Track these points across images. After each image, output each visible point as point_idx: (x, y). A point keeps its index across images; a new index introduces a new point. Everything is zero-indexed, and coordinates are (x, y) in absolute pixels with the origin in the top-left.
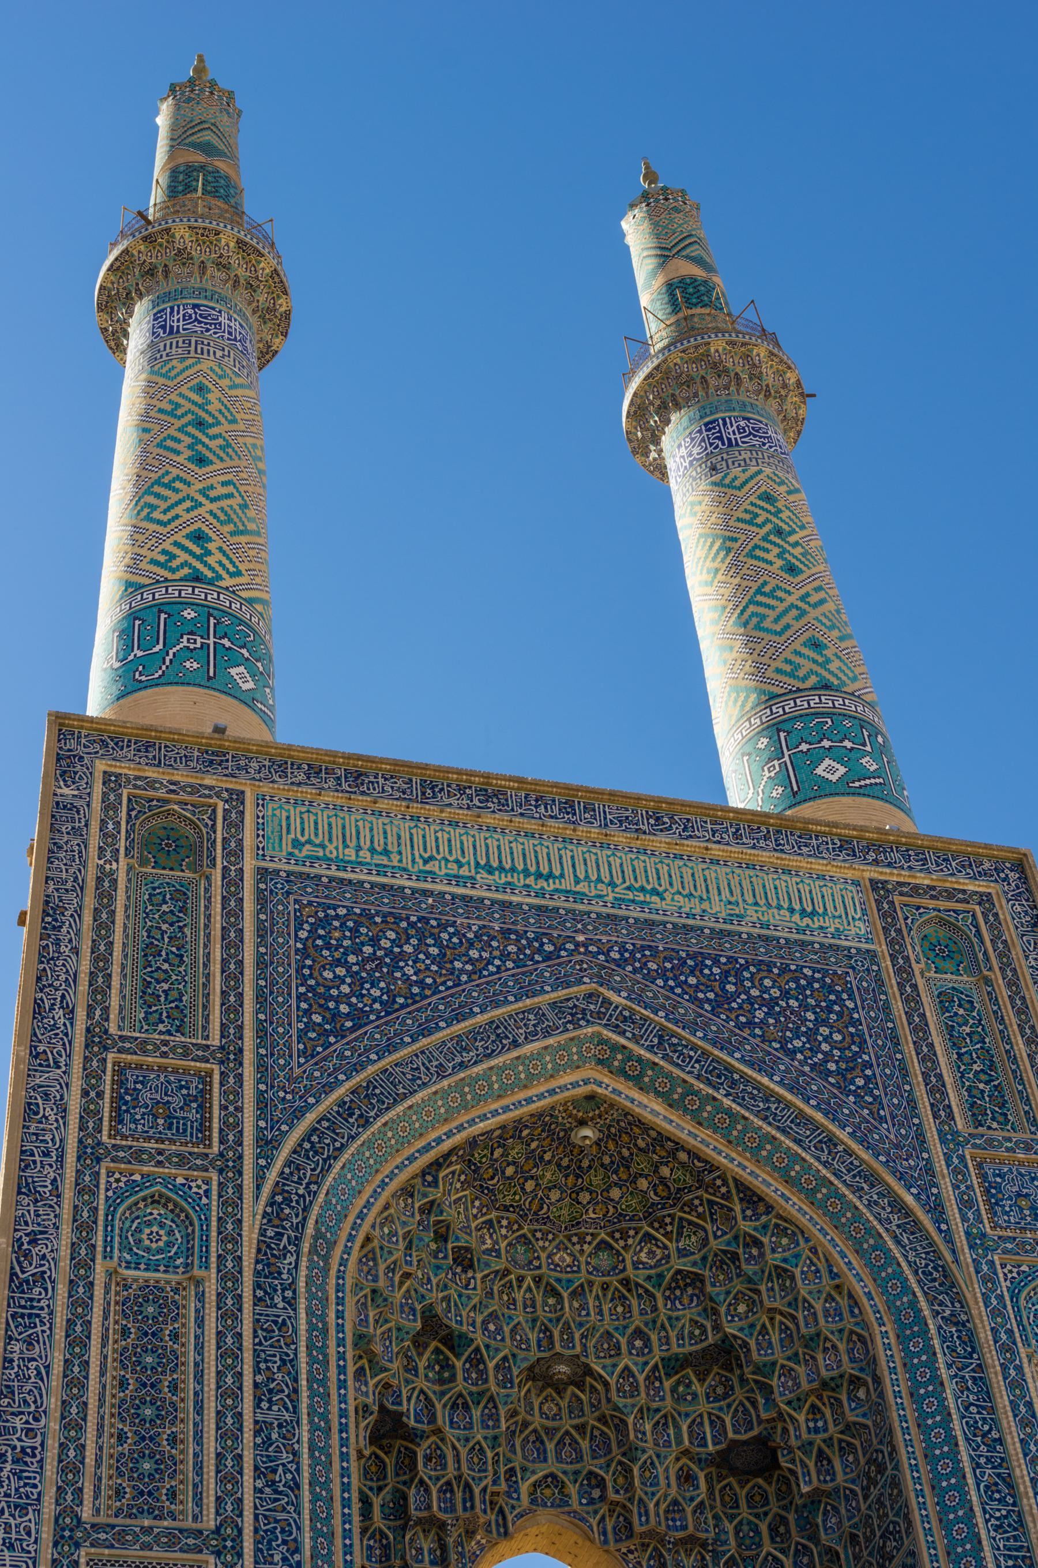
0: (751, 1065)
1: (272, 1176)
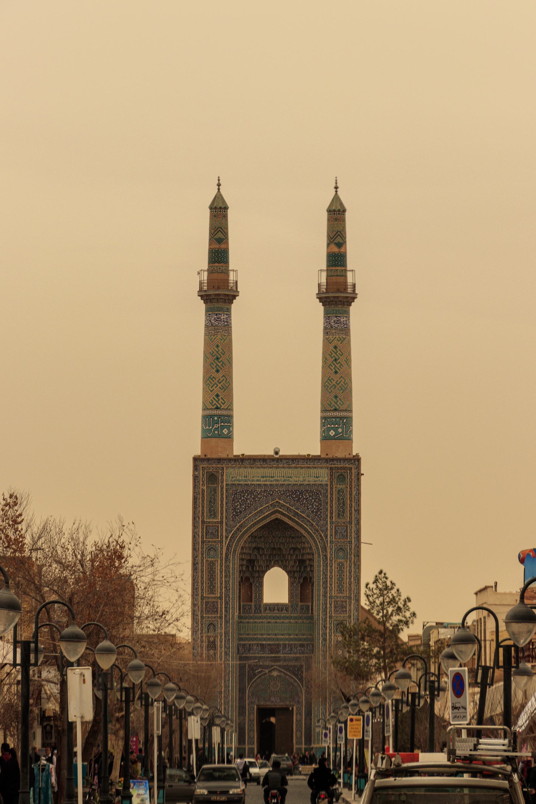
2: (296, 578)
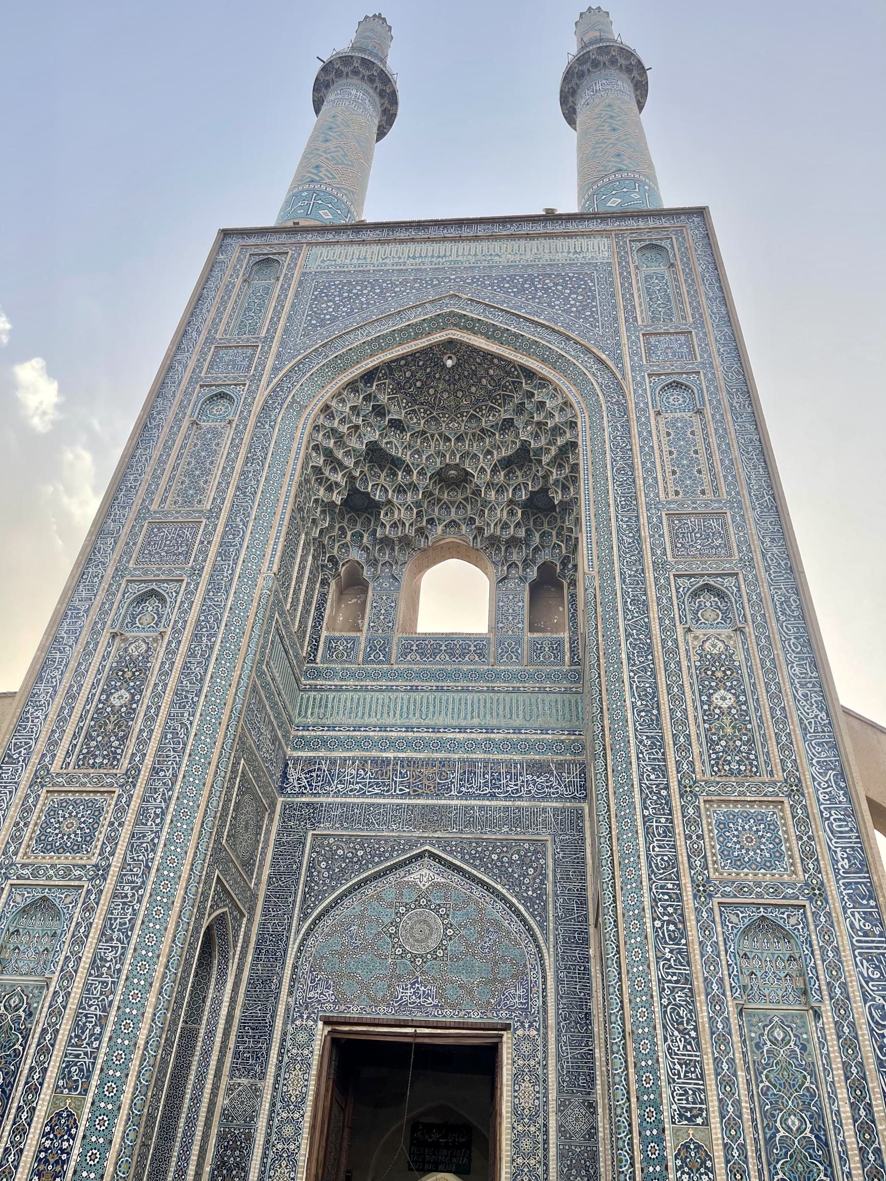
0: (530, 314)
1: (275, 381)
2: (514, 565)
